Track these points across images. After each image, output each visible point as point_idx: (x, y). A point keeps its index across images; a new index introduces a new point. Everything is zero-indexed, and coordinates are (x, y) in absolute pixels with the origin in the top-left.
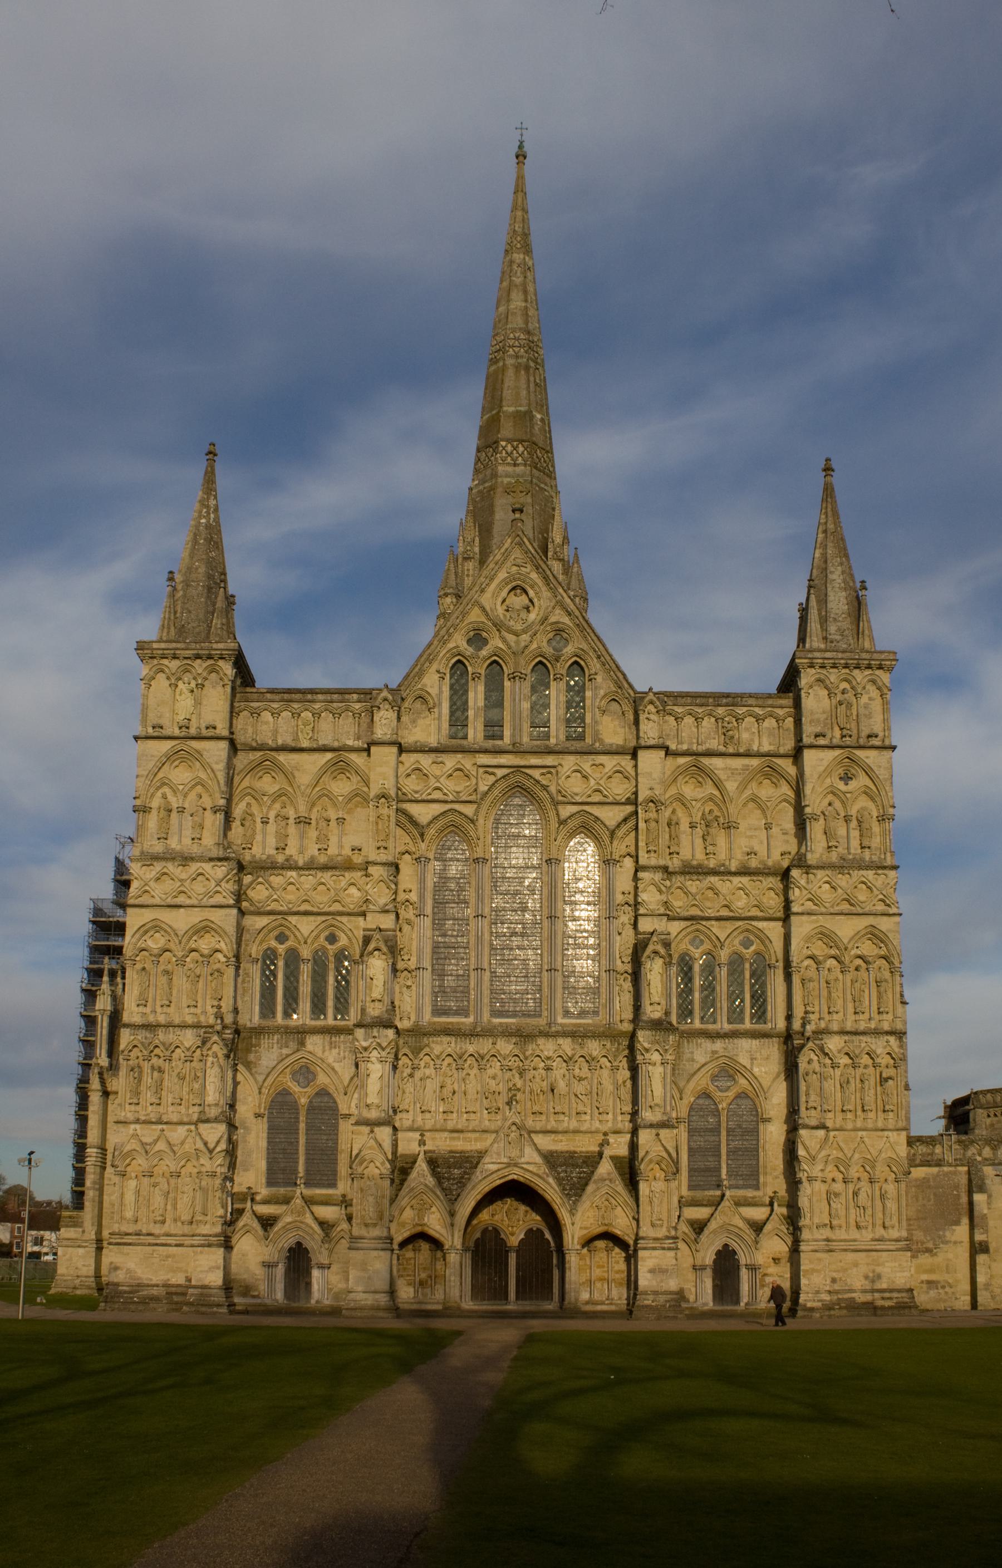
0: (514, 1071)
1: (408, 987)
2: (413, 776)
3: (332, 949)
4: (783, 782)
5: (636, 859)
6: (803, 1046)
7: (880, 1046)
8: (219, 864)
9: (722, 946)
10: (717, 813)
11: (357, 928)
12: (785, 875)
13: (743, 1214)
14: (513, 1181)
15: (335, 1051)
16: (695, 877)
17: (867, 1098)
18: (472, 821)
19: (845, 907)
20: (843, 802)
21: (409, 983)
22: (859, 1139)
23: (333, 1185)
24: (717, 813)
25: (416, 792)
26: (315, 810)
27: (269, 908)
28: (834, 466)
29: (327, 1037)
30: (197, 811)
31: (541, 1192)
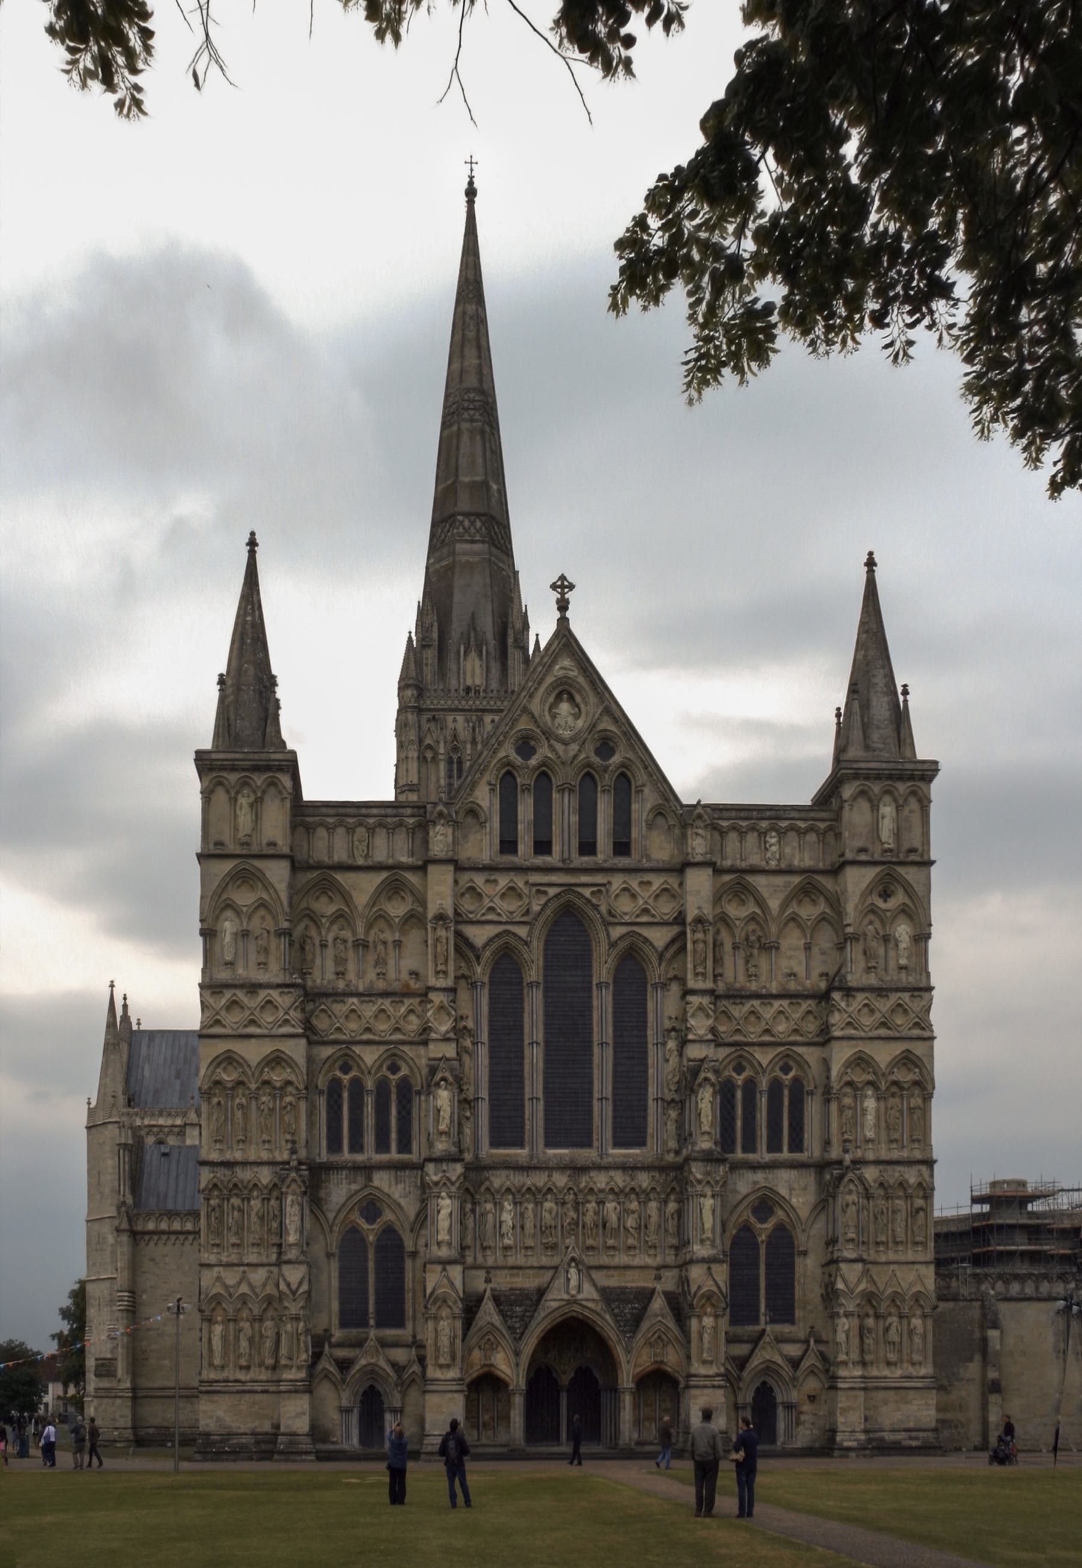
0: (569, 1205)
1: (468, 1118)
2: (467, 896)
3: (394, 1078)
4: (822, 900)
5: (681, 980)
6: (841, 1177)
7: (911, 1176)
8: (286, 990)
9: (764, 1071)
10: (759, 933)
11: (419, 1057)
12: (824, 997)
13: (785, 1352)
14: (572, 1318)
15: (401, 1186)
16: (738, 1001)
17: (899, 1230)
18: (526, 943)
19: (883, 1032)
20: (882, 921)
21: (468, 1114)
22: (890, 1272)
23: (401, 1324)
24: (759, 933)
25: (471, 913)
26: (372, 932)
27: (332, 1037)
28: (877, 560)
29: (393, 1173)
30: (261, 935)
31: (598, 1329)
